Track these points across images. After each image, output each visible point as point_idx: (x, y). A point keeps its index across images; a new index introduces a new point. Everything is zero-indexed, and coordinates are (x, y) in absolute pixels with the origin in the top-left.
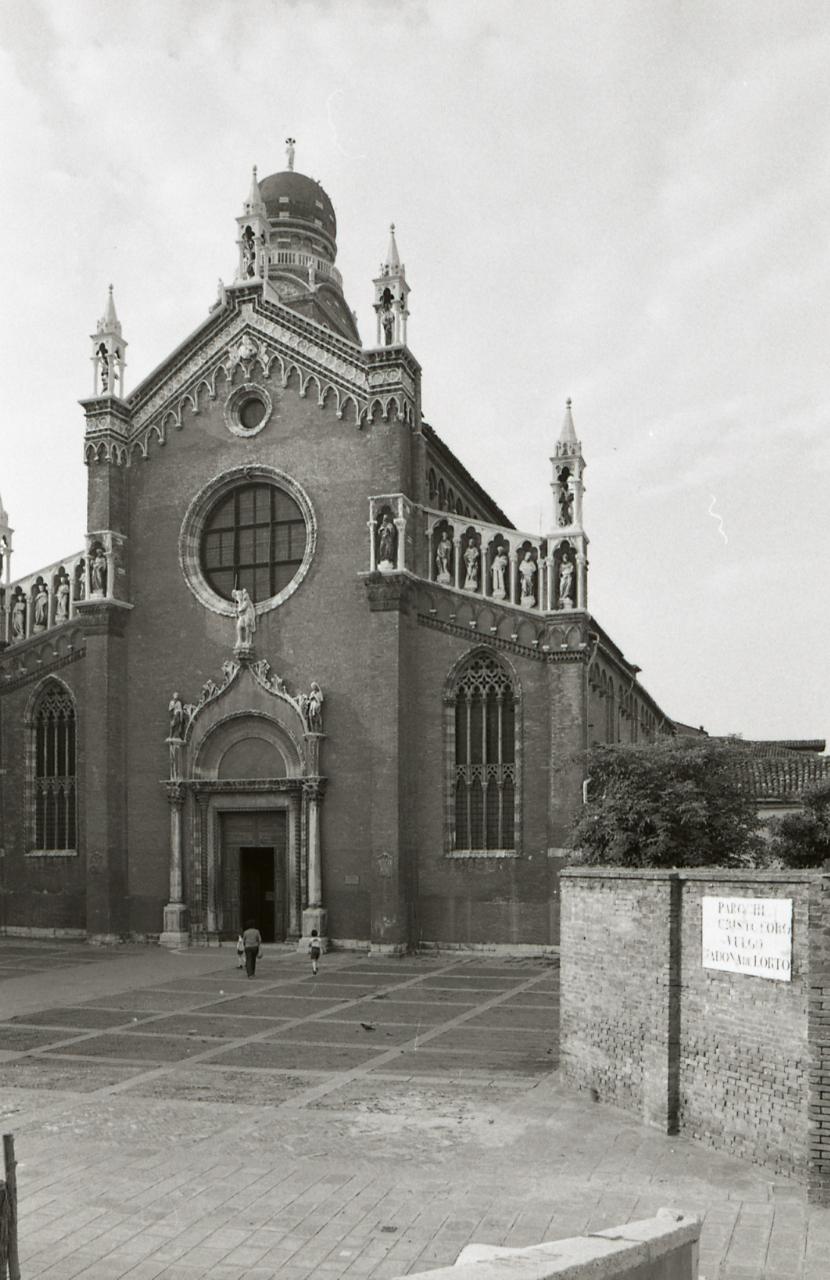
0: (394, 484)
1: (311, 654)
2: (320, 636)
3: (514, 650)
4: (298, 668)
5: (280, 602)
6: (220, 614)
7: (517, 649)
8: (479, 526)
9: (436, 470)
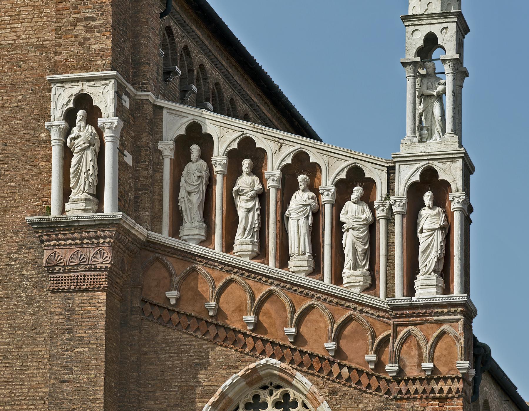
0: (100, 53)
3: (330, 373)
7: (335, 369)
8: (264, 138)
9: (177, 30)
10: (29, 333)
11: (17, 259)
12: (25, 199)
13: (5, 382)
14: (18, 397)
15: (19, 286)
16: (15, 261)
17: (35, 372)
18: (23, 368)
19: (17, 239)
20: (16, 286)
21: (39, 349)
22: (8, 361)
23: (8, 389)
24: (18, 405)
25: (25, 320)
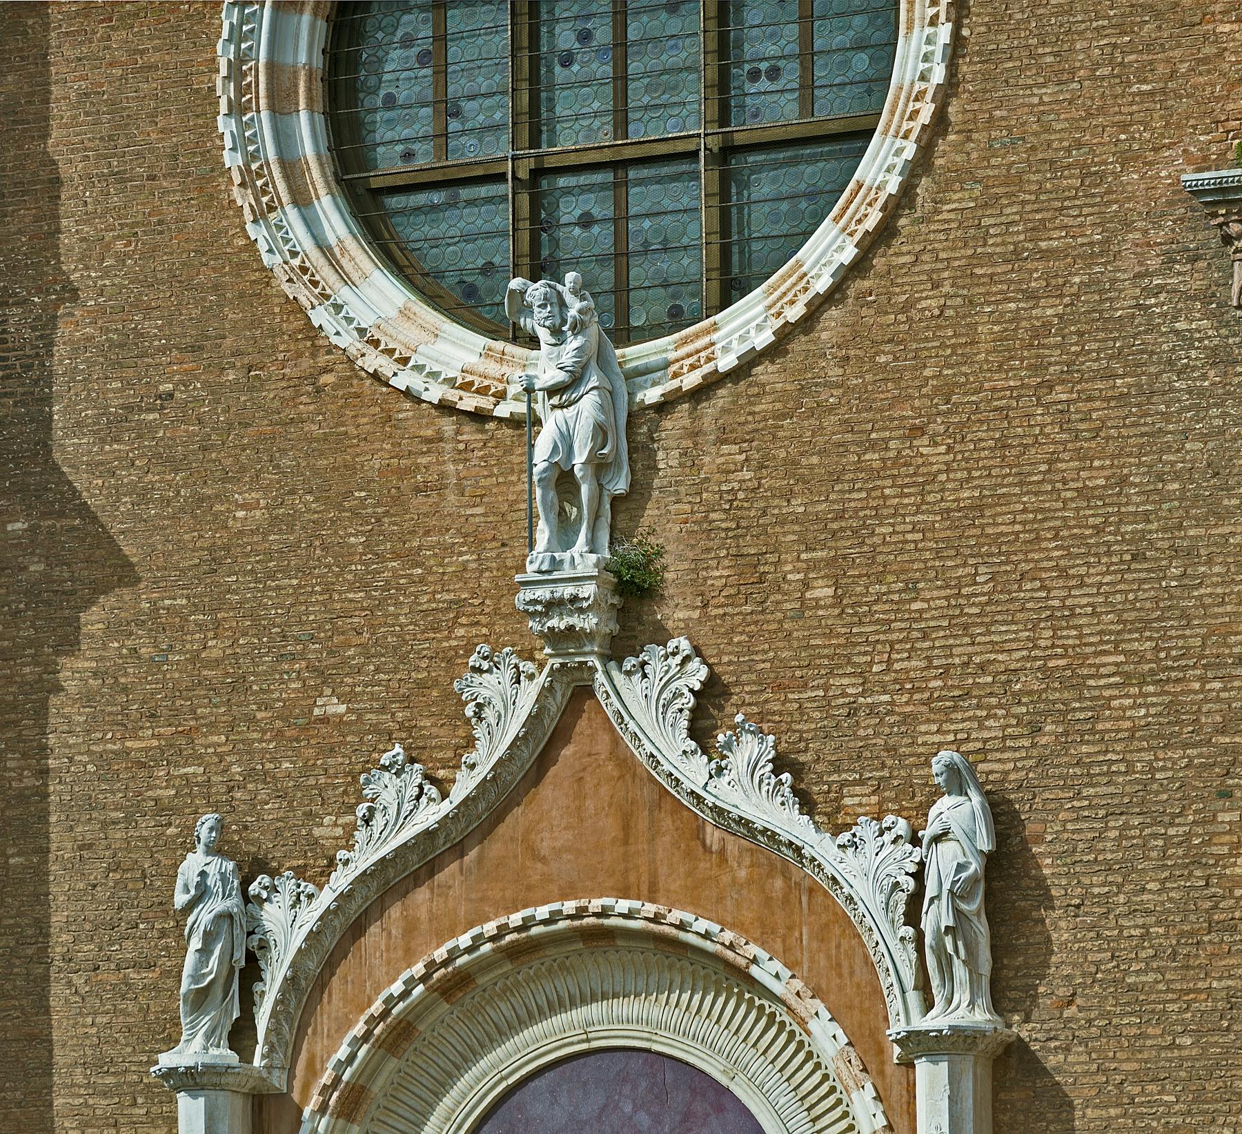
1: (932, 598)
2: (979, 507)
4: (863, 674)
5: (763, 339)
6: (445, 408)
10: (1199, 486)
11: (1161, 288)
12: (1179, 126)
13: (1141, 620)
14: (1175, 659)
15: (1170, 362)
16: (1156, 295)
17: (1219, 590)
18: (1186, 581)
19: (1159, 236)
20: (1159, 363)
21: (1227, 530)
22: (1146, 566)
23: (1150, 639)
24: (1178, 680)
25: (1187, 452)
